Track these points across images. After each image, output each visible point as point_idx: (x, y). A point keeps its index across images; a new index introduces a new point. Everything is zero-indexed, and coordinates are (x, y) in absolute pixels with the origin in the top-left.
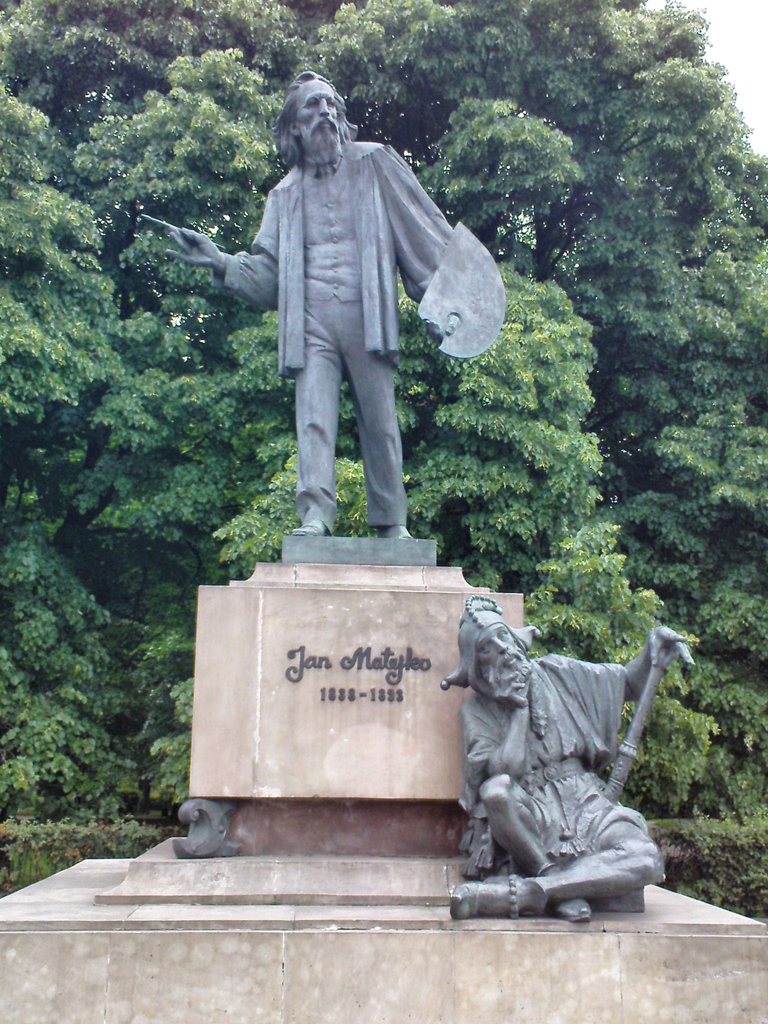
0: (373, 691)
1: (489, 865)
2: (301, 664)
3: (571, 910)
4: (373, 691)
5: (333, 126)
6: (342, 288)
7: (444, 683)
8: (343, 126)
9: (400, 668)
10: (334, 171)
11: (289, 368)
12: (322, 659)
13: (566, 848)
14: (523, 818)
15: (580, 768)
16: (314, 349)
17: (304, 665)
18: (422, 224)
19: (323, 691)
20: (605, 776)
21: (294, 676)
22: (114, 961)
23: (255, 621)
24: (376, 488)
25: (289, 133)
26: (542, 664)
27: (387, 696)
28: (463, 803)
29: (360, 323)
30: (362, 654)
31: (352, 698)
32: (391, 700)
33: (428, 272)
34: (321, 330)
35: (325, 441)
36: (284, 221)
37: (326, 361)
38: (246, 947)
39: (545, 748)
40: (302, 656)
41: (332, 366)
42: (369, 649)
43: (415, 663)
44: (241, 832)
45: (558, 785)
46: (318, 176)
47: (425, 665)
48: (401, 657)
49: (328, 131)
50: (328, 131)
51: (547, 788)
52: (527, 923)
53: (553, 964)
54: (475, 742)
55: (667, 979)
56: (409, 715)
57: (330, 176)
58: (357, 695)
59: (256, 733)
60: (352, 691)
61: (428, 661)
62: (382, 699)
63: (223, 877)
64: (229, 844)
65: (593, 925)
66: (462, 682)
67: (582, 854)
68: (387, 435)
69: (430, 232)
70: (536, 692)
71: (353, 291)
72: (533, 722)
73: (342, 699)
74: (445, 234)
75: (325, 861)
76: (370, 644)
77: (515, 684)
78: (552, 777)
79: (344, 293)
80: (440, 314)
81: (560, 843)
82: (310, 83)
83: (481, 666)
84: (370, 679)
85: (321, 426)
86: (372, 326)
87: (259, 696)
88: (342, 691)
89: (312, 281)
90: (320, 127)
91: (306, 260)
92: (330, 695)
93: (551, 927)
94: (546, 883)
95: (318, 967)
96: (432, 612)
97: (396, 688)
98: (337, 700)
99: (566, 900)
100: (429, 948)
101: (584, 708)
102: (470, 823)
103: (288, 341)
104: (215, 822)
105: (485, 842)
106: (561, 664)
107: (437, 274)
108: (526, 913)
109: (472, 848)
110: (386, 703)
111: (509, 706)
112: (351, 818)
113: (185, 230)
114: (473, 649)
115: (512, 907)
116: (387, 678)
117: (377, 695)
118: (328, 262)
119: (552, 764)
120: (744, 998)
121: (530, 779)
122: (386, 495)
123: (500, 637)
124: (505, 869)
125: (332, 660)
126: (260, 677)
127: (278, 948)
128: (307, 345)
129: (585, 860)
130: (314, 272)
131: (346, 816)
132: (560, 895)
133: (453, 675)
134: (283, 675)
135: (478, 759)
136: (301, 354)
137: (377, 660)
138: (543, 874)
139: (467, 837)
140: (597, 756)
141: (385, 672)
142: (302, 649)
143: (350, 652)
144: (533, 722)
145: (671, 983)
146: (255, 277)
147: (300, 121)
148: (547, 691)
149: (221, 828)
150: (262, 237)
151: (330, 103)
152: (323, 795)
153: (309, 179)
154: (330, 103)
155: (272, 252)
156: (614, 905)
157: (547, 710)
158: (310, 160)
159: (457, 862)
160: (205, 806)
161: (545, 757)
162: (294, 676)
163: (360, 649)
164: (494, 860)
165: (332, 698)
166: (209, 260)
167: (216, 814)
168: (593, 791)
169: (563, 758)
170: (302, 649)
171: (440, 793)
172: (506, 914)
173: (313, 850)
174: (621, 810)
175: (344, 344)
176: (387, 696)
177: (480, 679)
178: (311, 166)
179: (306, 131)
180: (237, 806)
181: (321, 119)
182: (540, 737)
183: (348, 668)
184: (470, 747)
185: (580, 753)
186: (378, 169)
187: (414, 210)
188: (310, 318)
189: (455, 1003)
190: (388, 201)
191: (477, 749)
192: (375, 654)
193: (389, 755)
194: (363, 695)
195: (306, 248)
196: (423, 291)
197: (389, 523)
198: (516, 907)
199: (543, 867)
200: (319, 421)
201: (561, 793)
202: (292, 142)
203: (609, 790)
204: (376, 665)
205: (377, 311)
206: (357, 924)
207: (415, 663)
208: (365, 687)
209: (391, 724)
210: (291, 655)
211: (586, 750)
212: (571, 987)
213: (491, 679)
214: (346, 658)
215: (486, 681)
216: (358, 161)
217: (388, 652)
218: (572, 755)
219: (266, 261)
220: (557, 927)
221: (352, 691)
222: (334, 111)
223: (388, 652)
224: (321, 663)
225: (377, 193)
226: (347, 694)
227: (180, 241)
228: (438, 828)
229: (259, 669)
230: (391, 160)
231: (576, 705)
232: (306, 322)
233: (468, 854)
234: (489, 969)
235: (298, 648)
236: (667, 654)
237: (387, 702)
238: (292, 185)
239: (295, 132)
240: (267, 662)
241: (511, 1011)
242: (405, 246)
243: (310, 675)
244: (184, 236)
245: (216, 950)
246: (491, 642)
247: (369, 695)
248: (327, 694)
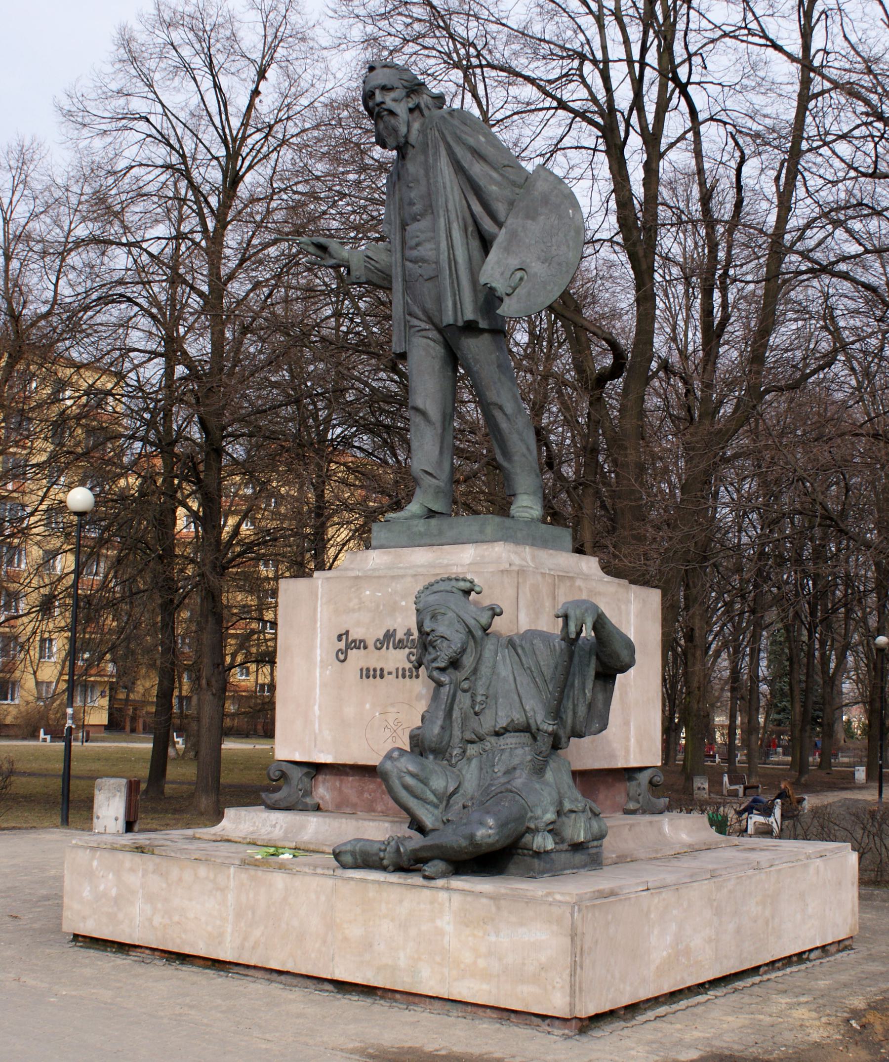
2: (348, 644)
4: (397, 669)
12: (361, 641)
17: (348, 647)
19: (361, 670)
21: (342, 656)
22: (143, 876)
23: (315, 609)
27: (407, 674)
30: (389, 635)
58: (385, 673)
59: (316, 708)
60: (382, 670)
65: (440, 882)
76: (395, 626)
77: (435, 665)
80: (502, 274)
92: (368, 674)
95: (251, 895)
107: (503, 230)
126: (319, 658)
127: (229, 877)
137: (400, 641)
141: (407, 651)
142: (347, 633)
143: (381, 635)
152: (361, 762)
162: (342, 656)
167: (296, 774)
169: (497, 734)
170: (347, 633)
183: (380, 649)
192: (400, 635)
194: (390, 673)
204: (400, 645)
214: (378, 640)
224: (360, 644)
226: (378, 673)
229: (318, 651)
232: (406, 304)
237: (407, 678)
240: (322, 646)
241: (371, 945)
243: (352, 653)
245: (196, 875)
247: (394, 674)
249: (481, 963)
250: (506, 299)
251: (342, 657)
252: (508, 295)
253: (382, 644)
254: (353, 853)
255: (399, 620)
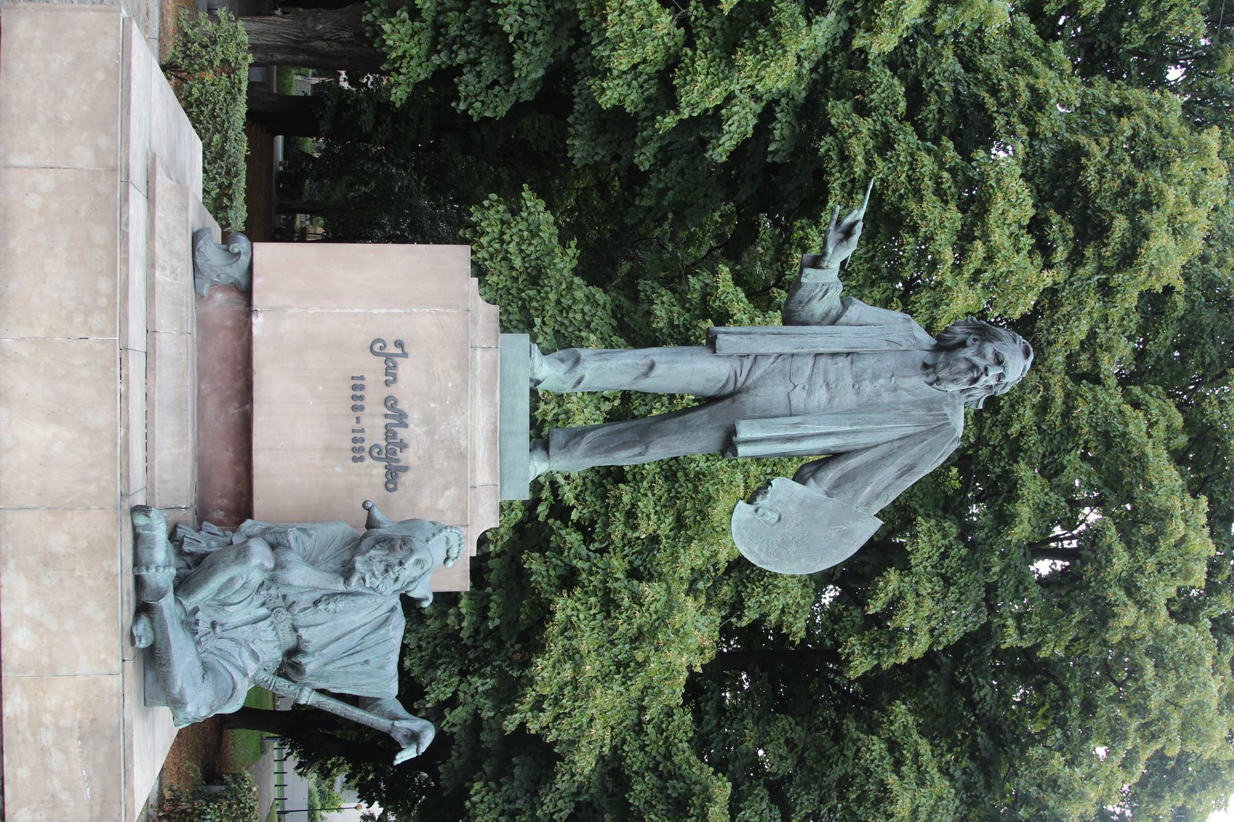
0: (362, 431)
1: (186, 548)
2: (389, 353)
3: (143, 627)
4: (362, 431)
5: (975, 380)
6: (804, 394)
7: (369, 505)
8: (980, 394)
9: (387, 459)
10: (931, 384)
11: (716, 337)
13: (203, 627)
14: (231, 580)
15: (287, 647)
16: (737, 364)
17: (389, 357)
18: (876, 479)
19: (362, 378)
20: (281, 673)
21: (376, 347)
24: (590, 436)
25: (969, 334)
26: (393, 609)
27: (358, 445)
28: (249, 522)
29: (766, 415)
30: (401, 418)
31: (354, 408)
32: (353, 450)
33: (825, 488)
34: (758, 373)
35: (637, 378)
36: (876, 331)
37: (725, 379)
38: (103, 301)
39: (305, 609)
40: (397, 355)
41: (720, 385)
42: (406, 426)
43: (393, 475)
44: (220, 297)
45: (267, 622)
46: (925, 366)
47: (391, 486)
48: (397, 461)
49: (970, 376)
50: (970, 376)
51: (263, 611)
52: (129, 583)
53: (90, 607)
54: (310, 536)
55: (80, 722)
56: (338, 469)
57: (925, 378)
58: (358, 413)
60: (362, 408)
61: (395, 489)
62: (355, 440)
63: (174, 278)
64: (207, 286)
65: (130, 650)
66: (371, 524)
67: (198, 643)
68: (647, 447)
69: (869, 489)
70: (361, 601)
71: (802, 406)
72: (332, 596)
73: (354, 398)
74: (868, 504)
75: (189, 381)
76: (412, 426)
78: (276, 617)
79: (799, 398)
81: (209, 621)
82: (1020, 355)
83: (387, 543)
84: (375, 426)
85: (653, 374)
86: (762, 427)
87: (356, 311)
88: (361, 398)
89: (811, 362)
90: (974, 367)
91: (834, 355)
92: (358, 386)
93: (126, 607)
94: (167, 604)
95: (85, 373)
96: (448, 493)
97: (366, 455)
98: (353, 393)
99: (152, 621)
100: (103, 483)
101: (351, 652)
102: (229, 533)
103: (745, 337)
104: (228, 270)
105: (209, 545)
106: (394, 628)
108: (139, 583)
109: (203, 533)
110: (351, 445)
111: (347, 572)
112: (234, 410)
113: (860, 225)
114: (406, 533)
115: (144, 568)
116: (376, 446)
117: (359, 435)
118: (832, 377)
119: (289, 616)
120: (64, 796)
121: (273, 592)
122: (583, 445)
123: (418, 562)
124: (182, 564)
125: (393, 386)
126: (375, 311)
127: (101, 333)
128: (742, 357)
129: (191, 646)
130: (822, 361)
131: (236, 405)
132: (157, 617)
133: (378, 514)
134: (377, 336)
135: (291, 538)
136: (730, 352)
137: (395, 435)
138: (177, 601)
139: (215, 529)
140: (299, 664)
141: (383, 444)
143: (403, 405)
144: (332, 596)
145: (76, 724)
146: (816, 300)
147: (980, 346)
148: (365, 612)
149: (222, 276)
150: (859, 309)
151: (1000, 377)
152: (255, 379)
153: (923, 356)
154: (1000, 377)
155: (843, 319)
156: (150, 675)
157: (346, 612)
158: (942, 356)
159: (190, 516)
160: (244, 260)
161: (296, 609)
162: (376, 347)
163: (406, 416)
164: (191, 554)
165: (354, 387)
166: (830, 250)
167: (236, 271)
168: (264, 658)
169: (295, 629)
171: (258, 504)
172: (137, 563)
173: (202, 373)
174: (244, 687)
175: (743, 397)
176: (358, 445)
177: (374, 539)
178: (935, 359)
179: (969, 353)
180: (245, 291)
181: (982, 368)
182: (316, 603)
184: (304, 530)
185: (302, 647)
186: (934, 431)
187: (891, 470)
188: (772, 360)
189: (52, 509)
190: (903, 442)
191: (304, 537)
192: (402, 433)
193: (297, 449)
195: (848, 354)
196: (804, 482)
197: (552, 450)
198: (144, 573)
199: (184, 602)
200: (658, 371)
201: (260, 624)
202: (960, 337)
203: (263, 676)
204: (389, 433)
205: (781, 433)
206: (125, 411)
207: (393, 475)
208: (366, 422)
209: (328, 449)
210: (399, 344)
211: (305, 654)
212: (70, 625)
213: (373, 553)
215: (373, 547)
216: (941, 409)
217: (403, 446)
218: (299, 637)
219: (834, 313)
220: (126, 613)
221: (362, 408)
222: (993, 382)
223: (403, 446)
225: (910, 431)
226: (358, 403)
227: (848, 220)
228: (225, 501)
229: (383, 311)
230: (944, 444)
231: (353, 643)
233: (199, 529)
234: (84, 544)
235: (406, 350)
236: (405, 736)
238: (915, 338)
239: (969, 342)
240: (391, 322)
241: (46, 565)
242: (852, 463)
244: (853, 225)
246: (412, 551)
247: (358, 427)
248: (359, 382)
249: (47, 719)
250: (751, 508)
251: (377, 348)
252: (756, 511)
253: (392, 408)
254: (148, 527)
255: (418, 431)
